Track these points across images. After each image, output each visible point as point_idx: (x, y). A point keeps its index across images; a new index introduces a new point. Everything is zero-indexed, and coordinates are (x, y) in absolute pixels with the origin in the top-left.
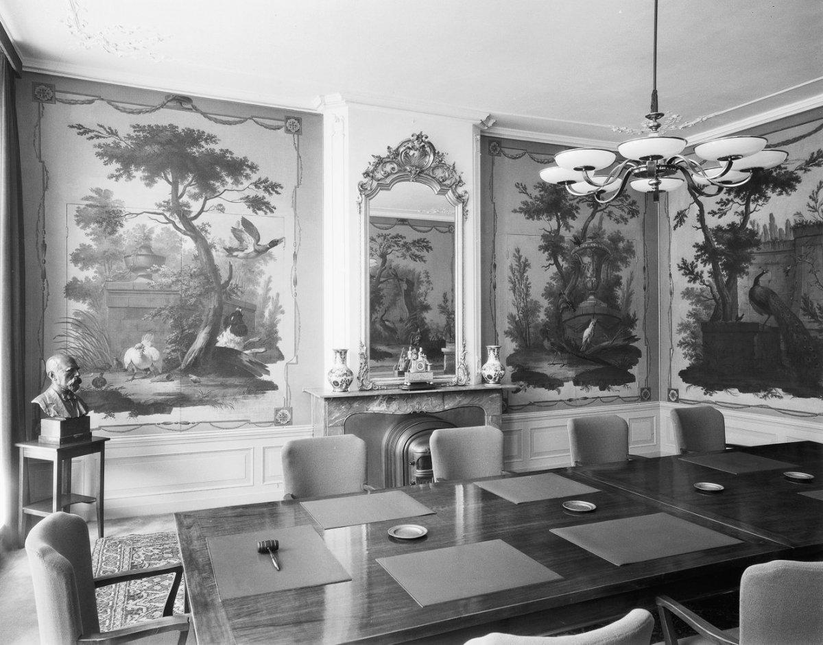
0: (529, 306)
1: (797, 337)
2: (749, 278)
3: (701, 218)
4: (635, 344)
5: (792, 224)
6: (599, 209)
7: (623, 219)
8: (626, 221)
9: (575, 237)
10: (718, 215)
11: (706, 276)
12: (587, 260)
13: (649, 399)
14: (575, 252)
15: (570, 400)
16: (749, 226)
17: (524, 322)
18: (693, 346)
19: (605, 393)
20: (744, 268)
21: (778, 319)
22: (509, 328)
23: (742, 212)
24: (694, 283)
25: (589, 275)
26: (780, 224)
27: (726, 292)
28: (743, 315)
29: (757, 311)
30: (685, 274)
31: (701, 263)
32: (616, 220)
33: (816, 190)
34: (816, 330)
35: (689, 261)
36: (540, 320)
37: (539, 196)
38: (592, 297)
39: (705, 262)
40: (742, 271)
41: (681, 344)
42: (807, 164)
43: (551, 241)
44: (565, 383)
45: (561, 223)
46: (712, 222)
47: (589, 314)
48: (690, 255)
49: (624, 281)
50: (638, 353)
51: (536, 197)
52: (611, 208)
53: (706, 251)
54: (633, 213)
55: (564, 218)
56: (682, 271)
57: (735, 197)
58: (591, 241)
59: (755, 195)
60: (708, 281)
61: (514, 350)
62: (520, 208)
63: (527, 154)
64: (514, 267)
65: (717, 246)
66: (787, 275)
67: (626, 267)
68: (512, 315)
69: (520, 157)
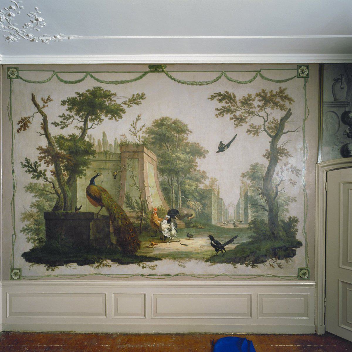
1: (122, 222)
2: (86, 178)
3: (45, 126)
5: (119, 142)
10: (60, 127)
11: (49, 175)
16: (87, 139)
18: (37, 232)
20: (82, 170)
21: (109, 210)
23: (81, 127)
24: (38, 179)
26: (111, 141)
27: (66, 188)
28: (81, 206)
29: (92, 203)
30: (30, 171)
31: (45, 163)
33: (135, 121)
34: (134, 217)
35: (33, 161)
39: (47, 163)
40: (81, 173)
41: (24, 230)
42: (130, 102)
46: (54, 131)
48: (34, 156)
53: (50, 154)
56: (26, 169)
57: (76, 114)
59: (92, 116)
60: (51, 179)
65: (59, 151)
66: (115, 178)
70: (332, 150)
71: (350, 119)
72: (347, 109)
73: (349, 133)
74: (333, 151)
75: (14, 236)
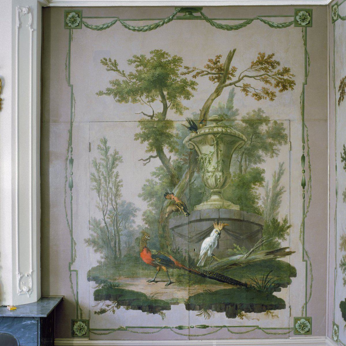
0: (120, 209)
4: (286, 259)
6: (228, 82)
7: (267, 93)
8: (272, 96)
9: (189, 121)
12: (207, 150)
13: (309, 332)
14: (190, 140)
15: (180, 328)
17: (112, 229)
19: (237, 321)
22: (91, 235)
25: (210, 168)
32: (256, 95)
36: (135, 226)
37: (134, 72)
38: (215, 197)
43: (153, 127)
44: (172, 306)
45: (168, 103)
47: (213, 220)
49: (268, 177)
50: (292, 272)
51: (131, 75)
52: (246, 81)
54: (285, 85)
55: (173, 97)
58: (214, 124)
61: (98, 262)
62: (108, 90)
63: (118, 22)
64: (98, 161)
67: (272, 157)
68: (95, 220)
69: (108, 27)
75: (336, 270)
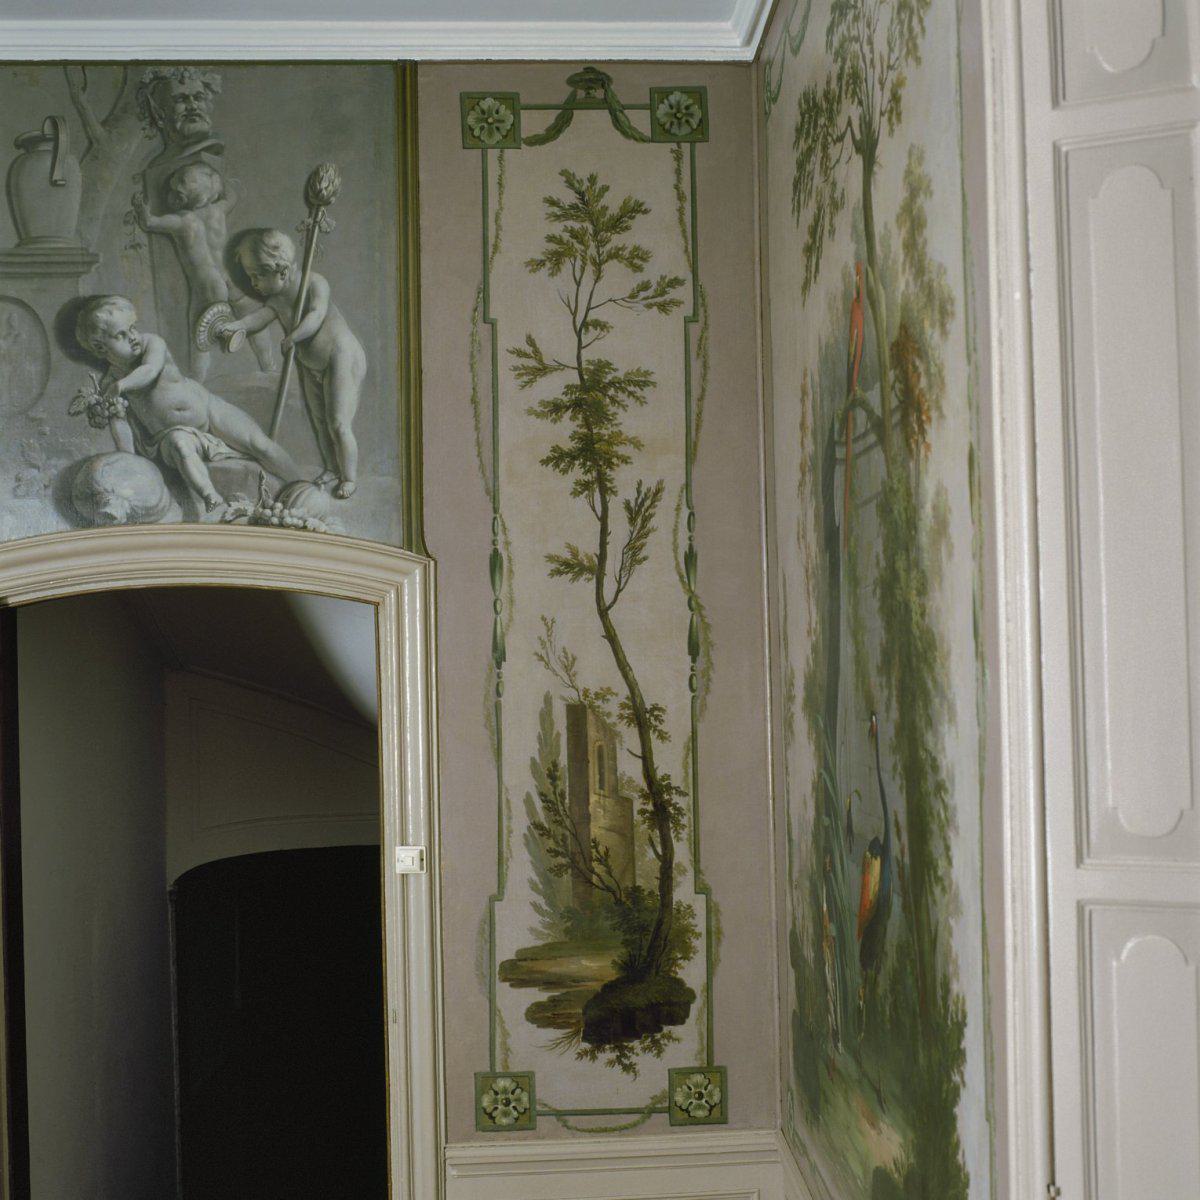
70: (15, 490)
71: (99, 336)
72: (85, 288)
73: (98, 403)
74: (16, 496)
